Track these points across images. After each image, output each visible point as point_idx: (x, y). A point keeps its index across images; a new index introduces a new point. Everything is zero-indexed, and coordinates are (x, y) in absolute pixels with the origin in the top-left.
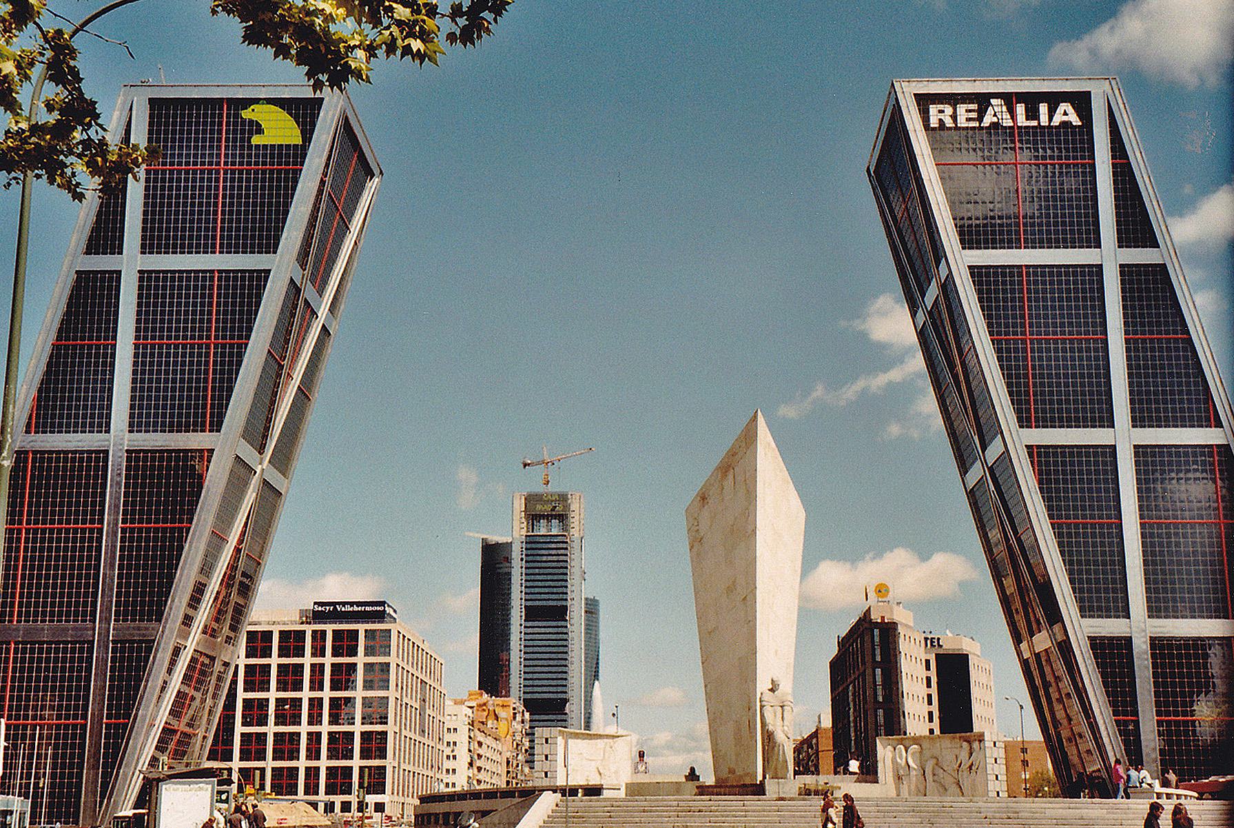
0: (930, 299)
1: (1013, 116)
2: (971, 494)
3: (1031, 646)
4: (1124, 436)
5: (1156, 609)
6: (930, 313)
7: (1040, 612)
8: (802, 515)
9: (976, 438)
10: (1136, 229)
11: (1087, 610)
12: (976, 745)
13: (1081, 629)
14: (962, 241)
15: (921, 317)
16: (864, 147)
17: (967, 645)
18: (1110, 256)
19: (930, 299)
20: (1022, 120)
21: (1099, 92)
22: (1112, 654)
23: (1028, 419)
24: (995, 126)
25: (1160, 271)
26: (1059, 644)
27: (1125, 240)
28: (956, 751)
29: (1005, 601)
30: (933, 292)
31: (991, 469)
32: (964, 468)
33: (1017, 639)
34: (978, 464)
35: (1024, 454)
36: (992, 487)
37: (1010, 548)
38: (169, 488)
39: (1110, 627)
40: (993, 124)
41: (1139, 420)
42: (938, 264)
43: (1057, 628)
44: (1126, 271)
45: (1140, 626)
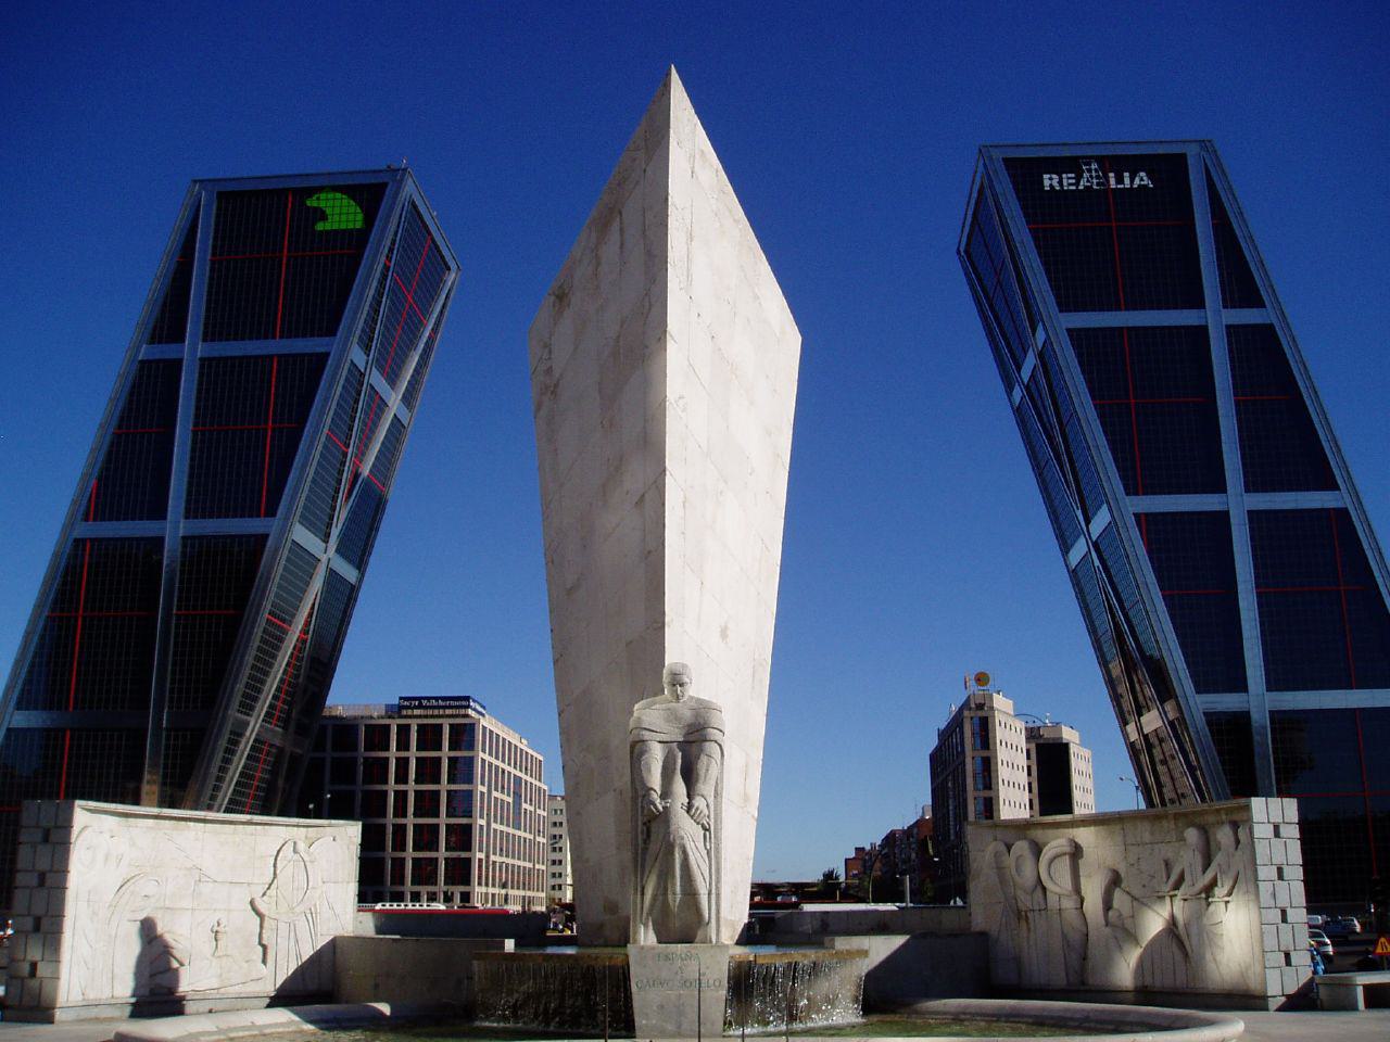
0: (1026, 374)
1: (1108, 181)
2: (1074, 574)
3: (1140, 729)
4: (1238, 502)
5: (1275, 683)
6: (1027, 387)
7: (1150, 691)
8: (793, 340)
9: (1079, 513)
10: (1242, 287)
11: (1202, 687)
12: (1224, 835)
13: (1200, 704)
14: (1059, 304)
15: (1017, 394)
16: (952, 229)
17: (1069, 735)
18: (1216, 317)
19: (1026, 374)
20: (1112, 181)
21: (1192, 151)
22: (1231, 731)
25: (1266, 334)
26: (1171, 724)
27: (1230, 302)
28: (1167, 851)
29: (1111, 683)
30: (1030, 362)
31: (1096, 545)
32: (1065, 548)
33: (1124, 722)
34: (1082, 540)
35: (1131, 521)
36: (1097, 563)
37: (1116, 625)
38: (230, 577)
39: (1228, 702)
40: (1086, 187)
42: (1034, 331)
43: (1169, 706)
44: (1232, 331)
45: (1259, 700)
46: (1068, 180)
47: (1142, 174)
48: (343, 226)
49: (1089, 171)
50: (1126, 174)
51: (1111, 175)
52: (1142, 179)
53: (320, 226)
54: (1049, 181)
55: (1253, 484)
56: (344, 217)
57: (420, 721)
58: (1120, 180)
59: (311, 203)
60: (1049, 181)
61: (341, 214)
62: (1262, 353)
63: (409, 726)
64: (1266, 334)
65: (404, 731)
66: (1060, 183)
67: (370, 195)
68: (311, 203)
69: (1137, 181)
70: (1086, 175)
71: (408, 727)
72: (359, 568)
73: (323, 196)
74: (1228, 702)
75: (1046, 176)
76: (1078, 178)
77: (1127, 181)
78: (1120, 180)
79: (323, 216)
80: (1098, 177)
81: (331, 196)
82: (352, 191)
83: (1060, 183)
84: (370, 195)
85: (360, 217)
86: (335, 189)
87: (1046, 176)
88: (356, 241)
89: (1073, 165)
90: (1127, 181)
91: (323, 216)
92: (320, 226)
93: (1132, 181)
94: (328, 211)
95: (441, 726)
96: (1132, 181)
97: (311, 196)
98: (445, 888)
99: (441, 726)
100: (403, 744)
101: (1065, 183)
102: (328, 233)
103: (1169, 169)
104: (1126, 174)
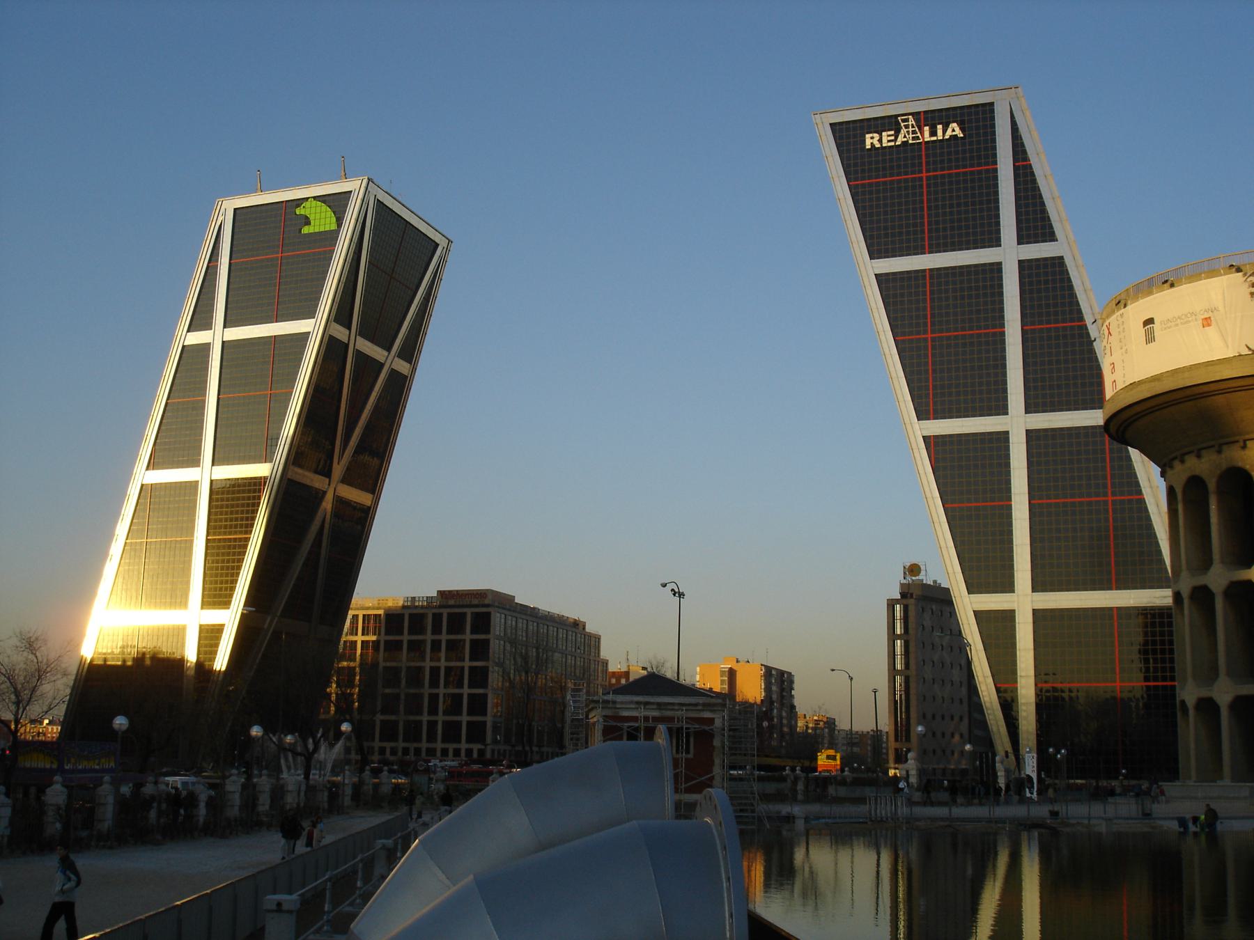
10: (1035, 223)
23: (927, 412)
27: (1024, 237)
41: (1031, 406)
46: (887, 138)
47: (954, 125)
48: (322, 229)
49: (907, 127)
50: (940, 127)
51: (927, 128)
52: (955, 129)
53: (306, 230)
54: (871, 140)
55: (1031, 406)
56: (323, 222)
57: (449, 610)
58: (933, 133)
60: (871, 140)
61: (321, 219)
62: (1049, 286)
63: (441, 614)
64: (1057, 266)
65: (437, 618)
66: (880, 141)
69: (949, 133)
70: (904, 131)
71: (441, 614)
72: (373, 493)
73: (307, 204)
74: (993, 602)
75: (868, 136)
77: (940, 132)
78: (933, 133)
79: (307, 221)
80: (914, 132)
83: (880, 141)
85: (334, 219)
87: (868, 136)
88: (331, 238)
89: (891, 123)
90: (940, 132)
91: (307, 221)
92: (306, 230)
93: (944, 132)
94: (312, 218)
95: (465, 614)
96: (944, 132)
97: (298, 206)
98: (467, 746)
99: (465, 614)
100: (437, 629)
101: (885, 140)
103: (978, 119)
104: (940, 127)
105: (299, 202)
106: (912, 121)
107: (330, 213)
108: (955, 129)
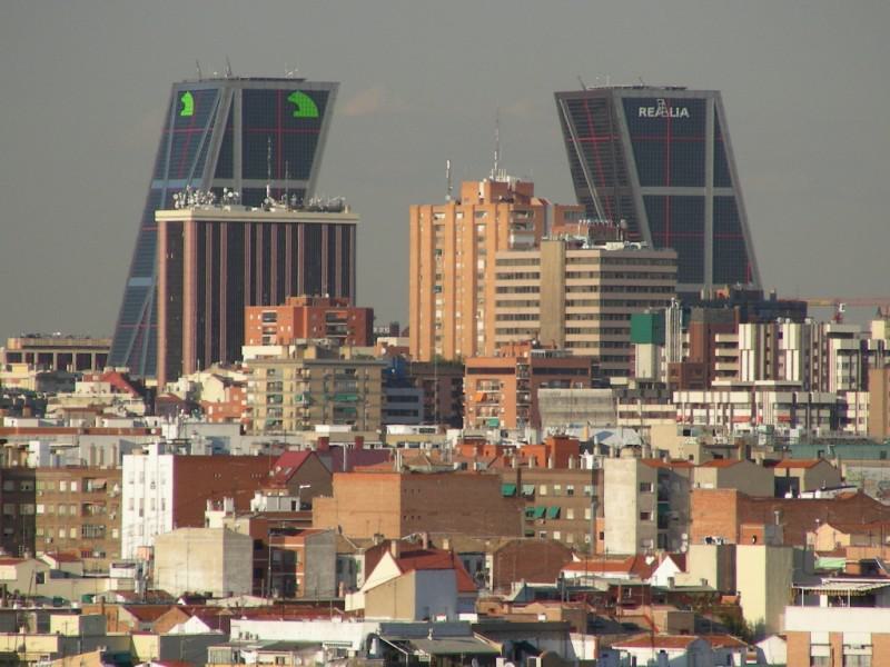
24: (659, 117)
52: (685, 112)
53: (296, 114)
54: (642, 111)
58: (674, 113)
59: (290, 99)
61: (307, 109)
67: (321, 97)
68: (290, 99)
70: (659, 108)
76: (656, 109)
78: (674, 113)
79: (296, 108)
81: (301, 95)
82: (310, 94)
84: (321, 97)
85: (316, 110)
86: (302, 91)
92: (296, 114)
94: (300, 106)
97: (290, 94)
101: (649, 112)
102: (300, 118)
103: (697, 105)
105: (289, 93)
106: (663, 103)
107: (313, 104)
108: (685, 112)
